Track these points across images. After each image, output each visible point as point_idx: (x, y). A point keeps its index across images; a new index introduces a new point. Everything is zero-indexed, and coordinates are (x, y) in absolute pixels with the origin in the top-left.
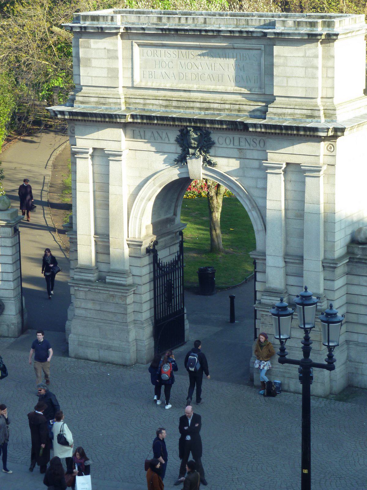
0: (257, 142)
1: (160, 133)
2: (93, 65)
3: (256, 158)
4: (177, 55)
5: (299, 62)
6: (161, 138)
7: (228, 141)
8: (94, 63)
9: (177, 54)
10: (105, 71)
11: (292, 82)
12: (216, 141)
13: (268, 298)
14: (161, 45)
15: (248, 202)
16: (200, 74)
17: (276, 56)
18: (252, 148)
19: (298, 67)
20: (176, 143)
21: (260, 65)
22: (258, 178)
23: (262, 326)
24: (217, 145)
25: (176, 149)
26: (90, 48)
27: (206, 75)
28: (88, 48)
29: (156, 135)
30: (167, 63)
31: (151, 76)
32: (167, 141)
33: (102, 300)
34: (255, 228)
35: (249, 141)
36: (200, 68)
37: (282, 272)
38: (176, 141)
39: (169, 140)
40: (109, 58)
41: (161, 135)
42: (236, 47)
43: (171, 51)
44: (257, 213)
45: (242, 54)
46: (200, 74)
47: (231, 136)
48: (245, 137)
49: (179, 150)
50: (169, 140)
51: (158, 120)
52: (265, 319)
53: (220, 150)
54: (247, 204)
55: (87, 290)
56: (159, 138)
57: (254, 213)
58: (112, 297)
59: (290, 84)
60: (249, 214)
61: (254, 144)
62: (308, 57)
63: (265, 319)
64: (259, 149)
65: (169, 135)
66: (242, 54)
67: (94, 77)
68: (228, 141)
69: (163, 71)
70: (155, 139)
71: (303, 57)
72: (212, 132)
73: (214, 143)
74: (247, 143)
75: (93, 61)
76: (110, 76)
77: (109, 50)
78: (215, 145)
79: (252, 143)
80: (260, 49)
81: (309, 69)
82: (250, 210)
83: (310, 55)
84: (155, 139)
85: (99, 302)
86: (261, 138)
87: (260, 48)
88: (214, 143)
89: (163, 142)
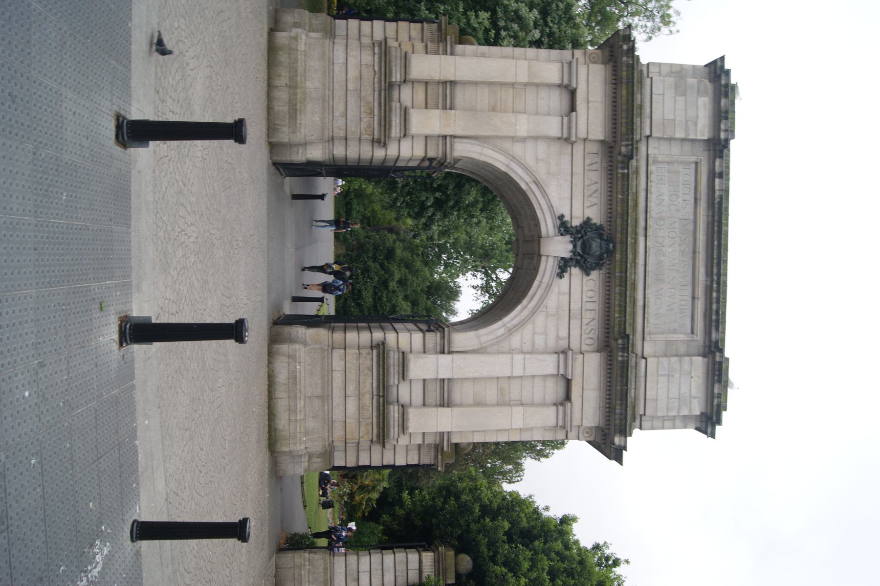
0: (591, 335)
1: (597, 194)
2: (678, 98)
3: (571, 333)
4: (684, 217)
5: (684, 390)
6: (590, 196)
7: (591, 294)
8: (681, 100)
9: (686, 217)
10: (671, 117)
11: (663, 380)
12: (591, 277)
13: (396, 362)
14: (698, 197)
15: (515, 322)
16: (664, 249)
17: (691, 360)
18: (584, 327)
19: (680, 389)
20: (585, 219)
21: (674, 332)
22: (546, 335)
23: (356, 353)
24: (586, 278)
25: (577, 218)
26: (698, 96)
27: (662, 258)
28: (698, 92)
29: (594, 188)
30: (675, 203)
31: (659, 178)
32: (587, 204)
33: (363, 94)
34: (482, 331)
35: (591, 324)
36: (670, 250)
37: (430, 376)
38: (589, 219)
39: (588, 207)
40: (686, 121)
41: (593, 195)
42: (696, 301)
43: (690, 208)
44: (502, 335)
45: (686, 307)
46: (664, 249)
47: (596, 299)
48: (597, 318)
49: (576, 222)
50: (588, 207)
51: (622, 199)
52: (365, 358)
53: (579, 282)
54: (512, 320)
55: (376, 69)
56: (591, 192)
57: (502, 331)
58: (369, 111)
59: (660, 379)
60: (500, 323)
61: (588, 331)
62: (690, 401)
63: (365, 358)
64: (583, 338)
65: (595, 207)
66: (686, 307)
67: (663, 99)
68: (591, 294)
69: (666, 198)
70: (588, 186)
71: (691, 396)
72: (601, 272)
73: (588, 274)
74: (589, 320)
75: (683, 98)
76: (665, 122)
77: (696, 124)
78: (584, 276)
79: (590, 328)
80: (692, 332)
81: (677, 404)
82: (504, 325)
83: (692, 404)
84: (588, 186)
85: (359, 87)
86: (596, 340)
87: (695, 332)
88: (588, 274)
89: (586, 198)
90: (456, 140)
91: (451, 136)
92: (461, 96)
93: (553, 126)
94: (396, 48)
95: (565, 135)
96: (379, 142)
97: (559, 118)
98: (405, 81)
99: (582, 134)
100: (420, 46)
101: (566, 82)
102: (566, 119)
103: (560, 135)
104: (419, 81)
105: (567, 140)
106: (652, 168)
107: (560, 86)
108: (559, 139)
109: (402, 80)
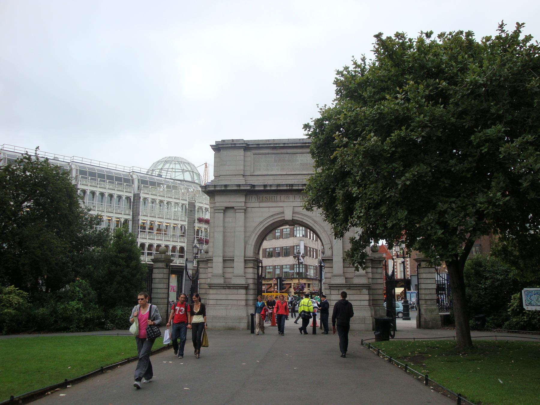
90: (246, 256)
91: (244, 258)
92: (229, 254)
93: (240, 216)
94: (211, 280)
95: (243, 211)
96: (247, 287)
97: (237, 213)
98: (223, 276)
99: (243, 204)
100: (209, 270)
101: (222, 211)
102: (237, 211)
103: (244, 213)
104: (223, 270)
105: (245, 210)
106: (255, 174)
107: (224, 213)
108: (245, 213)
109: (223, 277)
